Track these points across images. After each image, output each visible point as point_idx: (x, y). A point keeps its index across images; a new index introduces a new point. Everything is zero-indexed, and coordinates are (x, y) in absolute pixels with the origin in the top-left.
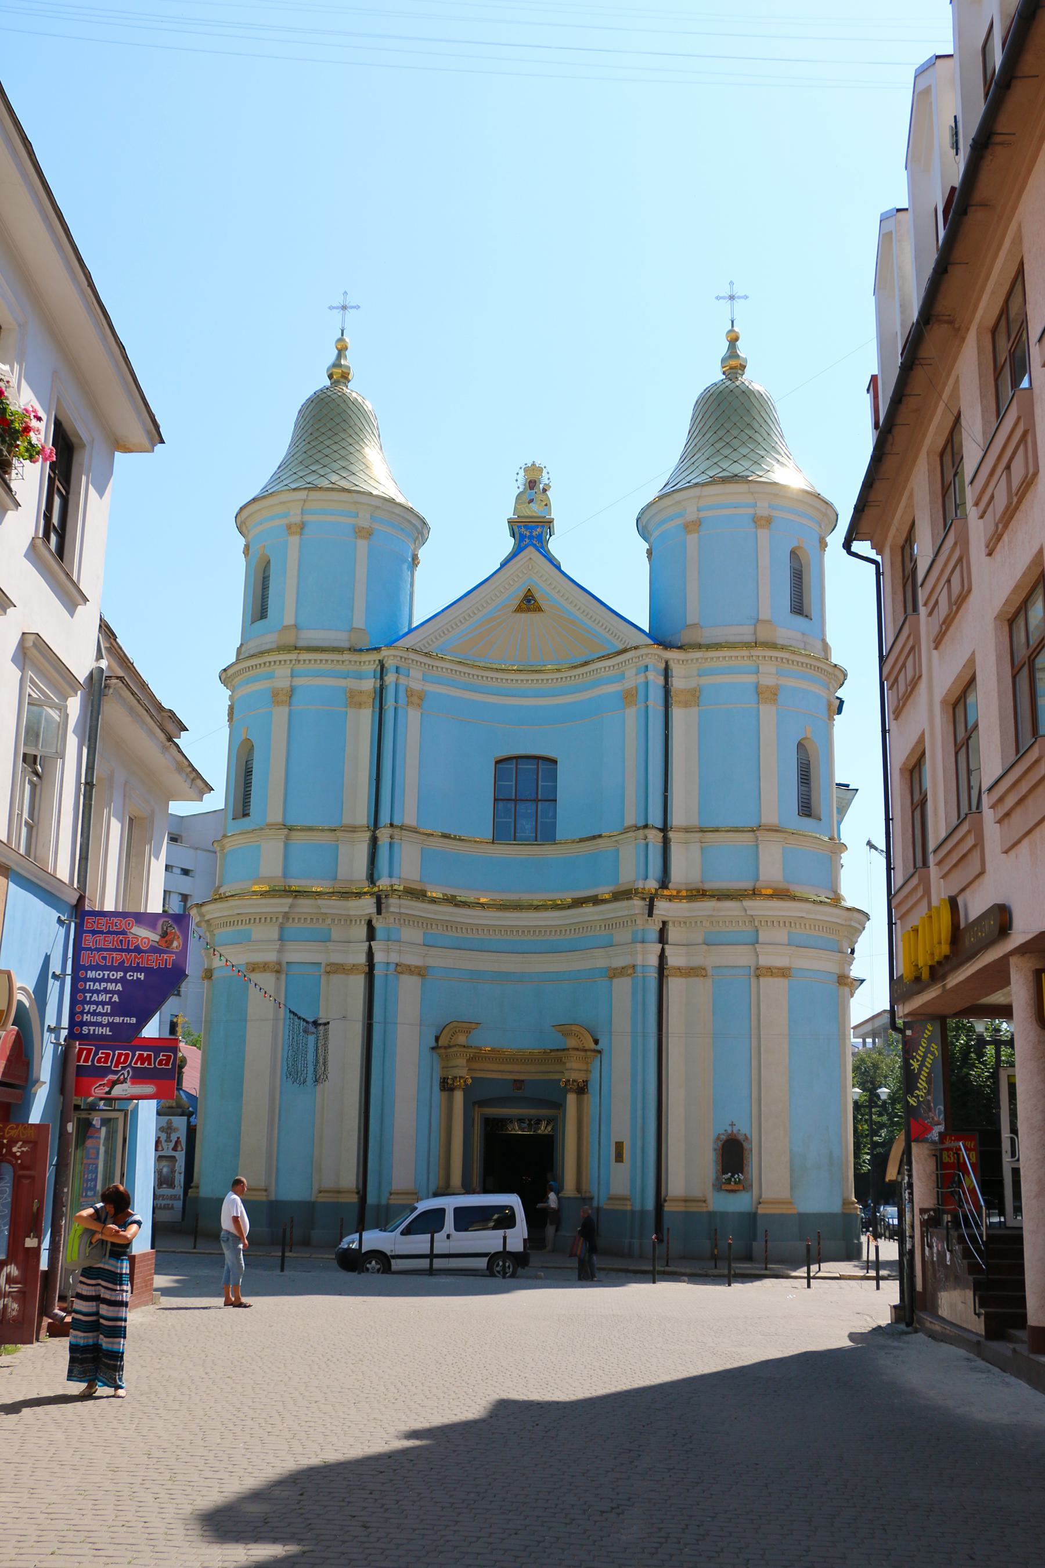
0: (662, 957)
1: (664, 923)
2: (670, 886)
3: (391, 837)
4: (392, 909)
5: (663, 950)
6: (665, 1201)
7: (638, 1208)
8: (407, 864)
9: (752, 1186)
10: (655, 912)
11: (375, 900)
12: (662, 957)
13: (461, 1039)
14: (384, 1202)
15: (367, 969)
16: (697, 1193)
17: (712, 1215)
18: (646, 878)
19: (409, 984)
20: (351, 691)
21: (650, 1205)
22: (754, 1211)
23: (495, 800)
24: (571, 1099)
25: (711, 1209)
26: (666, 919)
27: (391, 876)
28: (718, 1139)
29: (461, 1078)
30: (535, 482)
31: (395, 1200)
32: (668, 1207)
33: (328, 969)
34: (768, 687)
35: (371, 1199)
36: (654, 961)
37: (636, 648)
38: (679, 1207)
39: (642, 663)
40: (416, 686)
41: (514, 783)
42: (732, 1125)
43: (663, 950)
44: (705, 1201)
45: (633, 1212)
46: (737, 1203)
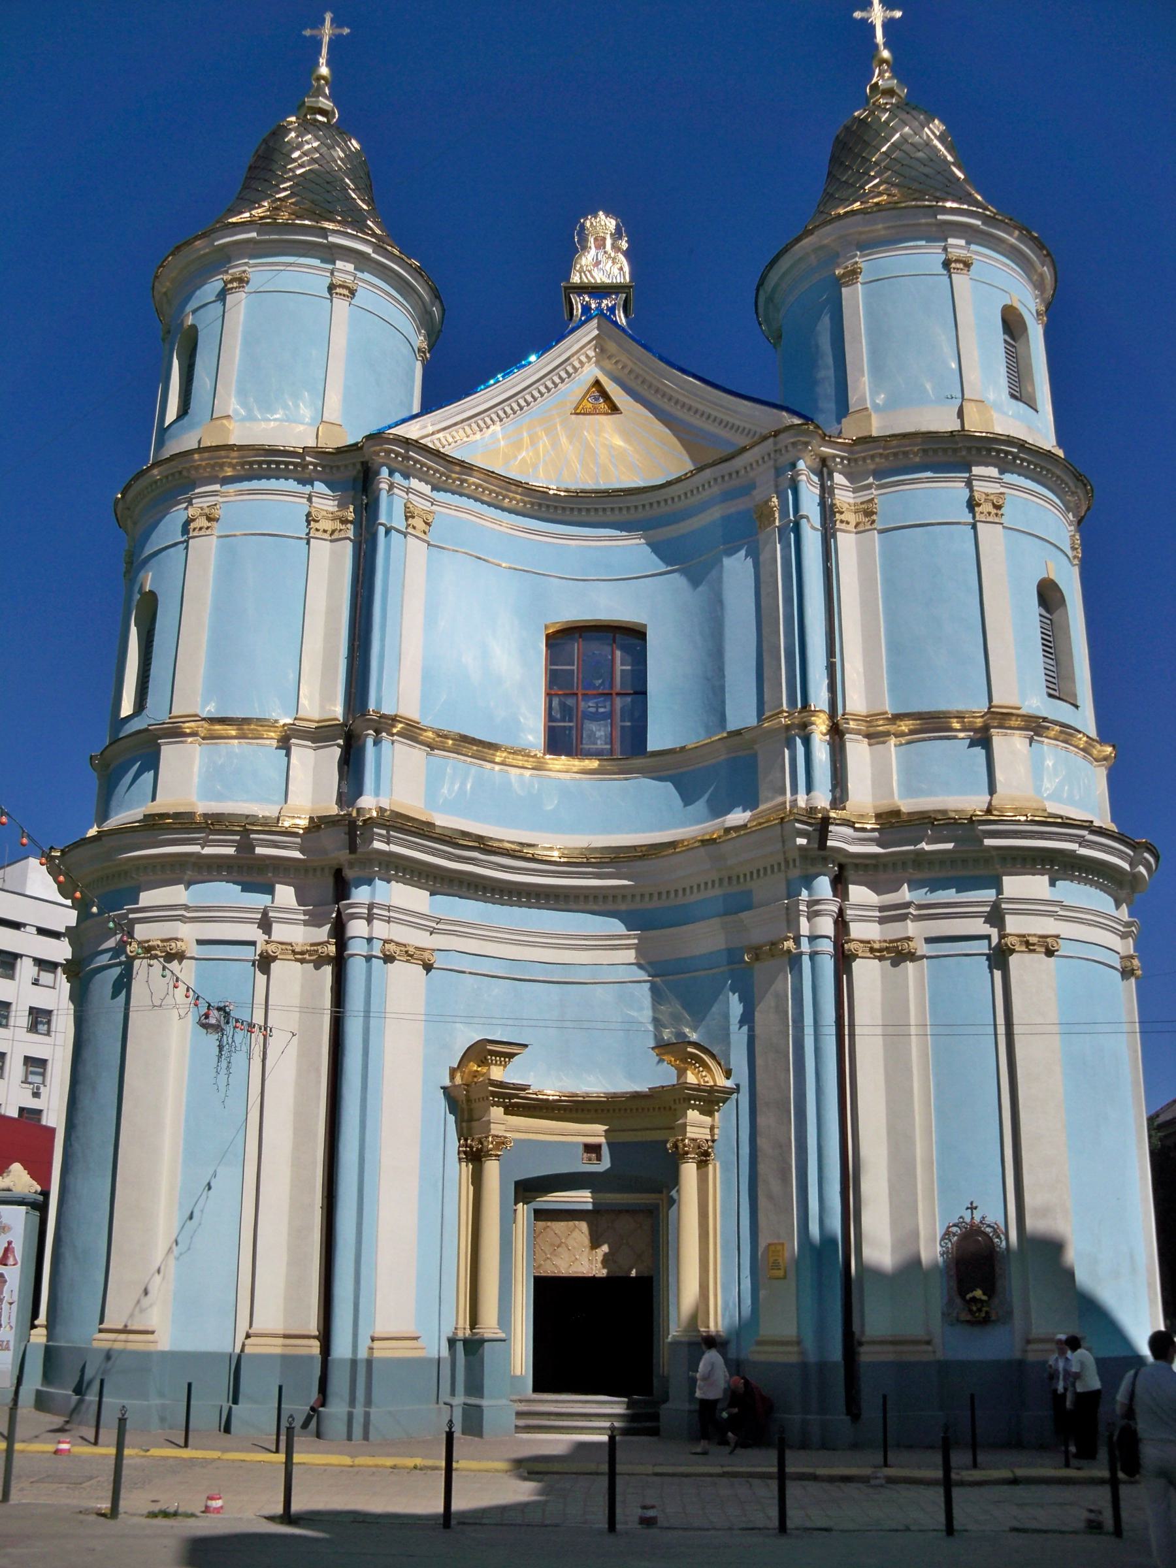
0: (841, 923)
1: (841, 867)
2: (848, 804)
3: (378, 732)
4: (377, 845)
5: (841, 912)
6: (861, 1344)
7: (812, 1358)
8: (401, 781)
9: (1010, 1313)
10: (829, 843)
11: (346, 829)
12: (841, 923)
13: (497, 1073)
14: (363, 1354)
15: (332, 950)
16: (916, 1331)
17: (944, 1367)
18: (809, 789)
19: (404, 974)
20: (319, 510)
21: (836, 1354)
22: (1018, 1355)
23: (549, 695)
24: (689, 1170)
25: (939, 1356)
26: (843, 860)
27: (377, 793)
28: (947, 1234)
29: (494, 1136)
30: (604, 239)
31: (382, 1351)
32: (866, 1355)
33: (271, 948)
34: (987, 495)
35: (341, 1348)
36: (826, 926)
37: (777, 434)
38: (887, 1355)
39: (785, 459)
40: (420, 504)
41: (575, 667)
42: (972, 1208)
43: (841, 912)
44: (928, 1343)
45: (804, 1366)
46: (990, 1346)
